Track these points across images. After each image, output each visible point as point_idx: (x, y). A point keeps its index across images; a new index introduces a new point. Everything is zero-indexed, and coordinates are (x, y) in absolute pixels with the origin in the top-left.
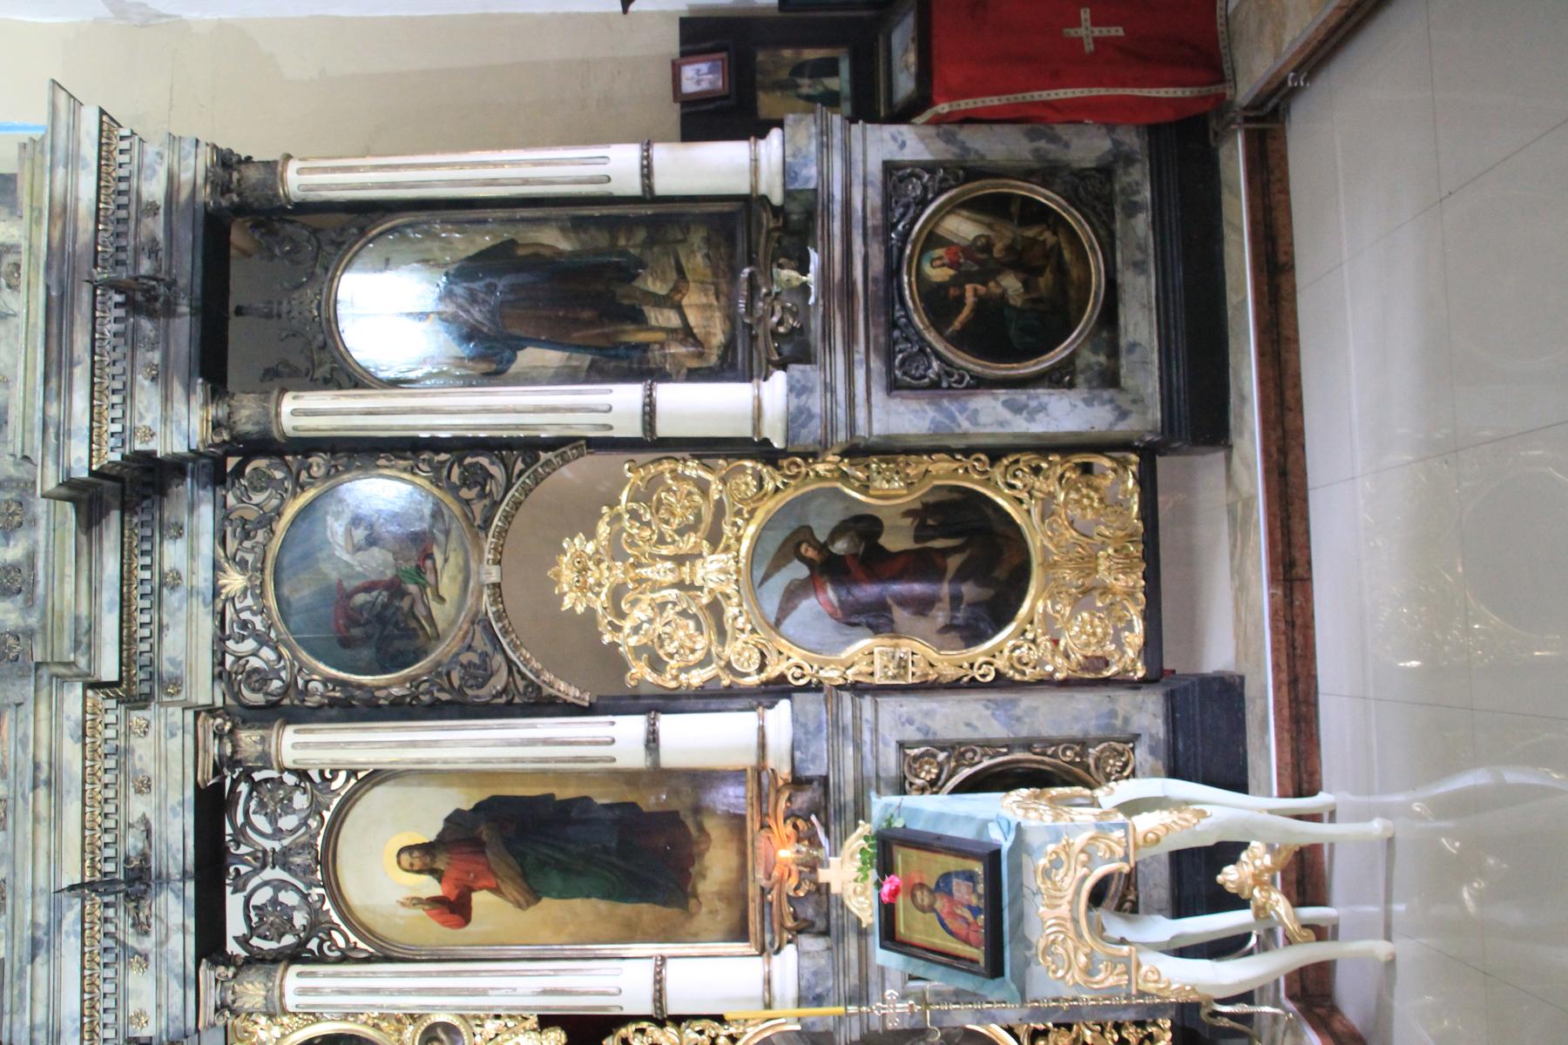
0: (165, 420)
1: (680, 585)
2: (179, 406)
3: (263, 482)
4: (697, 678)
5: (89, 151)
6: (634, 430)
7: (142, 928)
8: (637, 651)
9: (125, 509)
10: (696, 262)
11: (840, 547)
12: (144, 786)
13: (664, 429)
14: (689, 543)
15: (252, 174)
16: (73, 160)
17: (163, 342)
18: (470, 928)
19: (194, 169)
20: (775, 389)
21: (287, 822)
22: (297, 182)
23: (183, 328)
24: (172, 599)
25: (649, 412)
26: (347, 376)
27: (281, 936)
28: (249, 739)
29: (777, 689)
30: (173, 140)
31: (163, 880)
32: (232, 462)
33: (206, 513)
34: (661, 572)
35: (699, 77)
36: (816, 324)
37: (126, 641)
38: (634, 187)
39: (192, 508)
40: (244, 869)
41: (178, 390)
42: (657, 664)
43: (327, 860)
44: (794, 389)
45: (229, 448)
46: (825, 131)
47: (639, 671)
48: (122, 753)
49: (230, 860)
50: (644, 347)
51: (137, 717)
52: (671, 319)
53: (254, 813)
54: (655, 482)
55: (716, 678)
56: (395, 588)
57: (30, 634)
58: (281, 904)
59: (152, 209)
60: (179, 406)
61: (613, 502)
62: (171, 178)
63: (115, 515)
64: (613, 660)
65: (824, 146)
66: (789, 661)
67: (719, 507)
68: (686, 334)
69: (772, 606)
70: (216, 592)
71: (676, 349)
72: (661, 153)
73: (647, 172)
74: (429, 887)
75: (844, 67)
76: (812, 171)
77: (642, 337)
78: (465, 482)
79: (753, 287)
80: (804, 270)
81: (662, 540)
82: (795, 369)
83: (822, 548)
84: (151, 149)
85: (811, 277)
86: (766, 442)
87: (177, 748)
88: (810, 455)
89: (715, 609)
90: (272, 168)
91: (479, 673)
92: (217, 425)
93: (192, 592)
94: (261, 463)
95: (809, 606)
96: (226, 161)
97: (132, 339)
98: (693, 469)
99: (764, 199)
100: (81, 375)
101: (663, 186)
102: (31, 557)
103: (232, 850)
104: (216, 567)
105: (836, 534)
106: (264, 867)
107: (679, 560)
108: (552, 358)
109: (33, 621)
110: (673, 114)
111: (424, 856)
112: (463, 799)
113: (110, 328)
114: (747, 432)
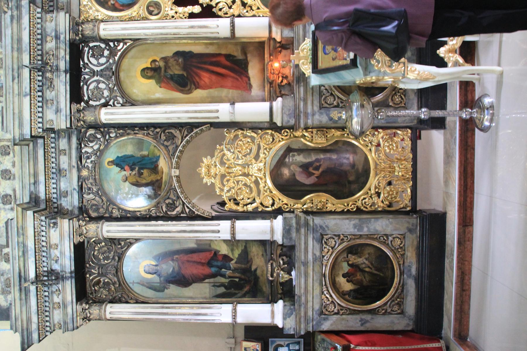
21: (103, 60)
27: (100, 99)
40: (87, 77)
43: (116, 74)
49: (83, 73)
53: (91, 57)
58: (99, 88)
103: (83, 70)
106: (94, 76)
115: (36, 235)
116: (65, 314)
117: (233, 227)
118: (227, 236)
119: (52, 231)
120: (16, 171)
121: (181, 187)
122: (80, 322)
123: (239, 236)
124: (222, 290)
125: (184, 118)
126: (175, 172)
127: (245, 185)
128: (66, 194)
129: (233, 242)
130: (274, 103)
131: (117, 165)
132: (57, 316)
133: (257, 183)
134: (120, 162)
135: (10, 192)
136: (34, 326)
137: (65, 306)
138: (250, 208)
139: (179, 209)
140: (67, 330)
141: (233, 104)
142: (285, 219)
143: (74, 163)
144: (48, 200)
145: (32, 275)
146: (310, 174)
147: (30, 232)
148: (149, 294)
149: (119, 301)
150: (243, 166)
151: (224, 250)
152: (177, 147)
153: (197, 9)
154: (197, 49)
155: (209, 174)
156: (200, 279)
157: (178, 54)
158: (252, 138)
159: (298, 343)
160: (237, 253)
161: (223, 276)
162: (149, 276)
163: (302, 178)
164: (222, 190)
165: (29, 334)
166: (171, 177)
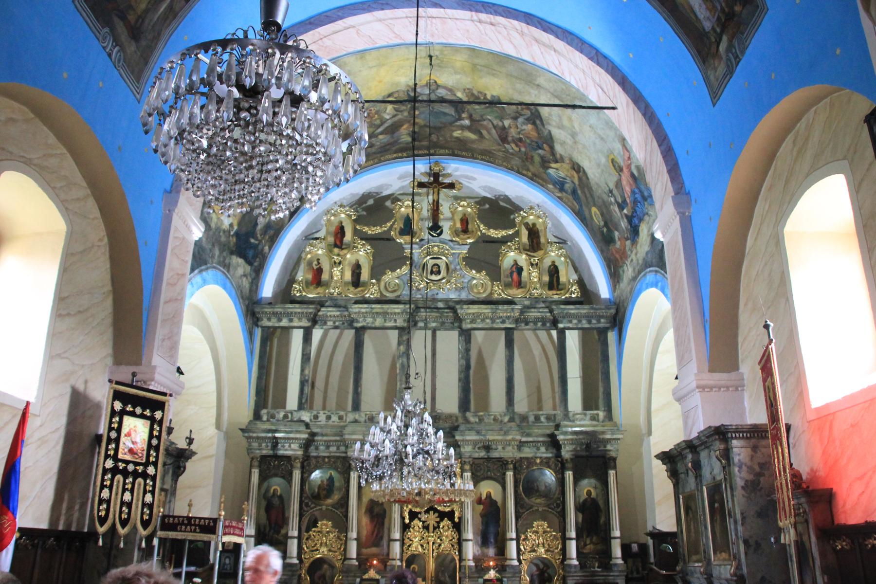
0: (568, 451)
1: (539, 544)
2: (570, 453)
3: (556, 465)
4: (522, 547)
5: (615, 437)
6: (567, 536)
7: (479, 448)
8: (527, 537)
9: (551, 441)
10: (599, 547)
11: (546, 575)
12: (504, 448)
13: (567, 542)
14: (546, 546)
15: (612, 464)
16: (613, 434)
17: (581, 450)
18: (476, 505)
19: (613, 454)
20: (575, 562)
22: (612, 473)
23: (584, 453)
24: (535, 449)
25: (571, 539)
26: (576, 481)
28: (511, 466)
29: (520, 562)
30: (617, 450)
31: (488, 452)
32: (559, 459)
33: (550, 455)
34: (541, 540)
35: (635, 547)
36: (588, 570)
37: (527, 442)
38: (612, 535)
39: (552, 453)
41: (573, 453)
42: (524, 540)
44: (575, 566)
45: (562, 460)
46: (622, 571)
47: (523, 537)
48: (509, 445)
50: (583, 537)
51: (516, 447)
52: (588, 542)
54: (557, 540)
55: (521, 550)
56: (538, 491)
57: (528, 422)
59: (605, 447)
60: (570, 453)
61: (554, 531)
62: (610, 450)
63: (549, 439)
64: (525, 532)
65: (620, 571)
66: (525, 567)
67: (553, 552)
68: (585, 545)
69: (535, 561)
70: (537, 458)
71: (582, 544)
72: (618, 541)
73: (615, 538)
74: (484, 496)
75: (638, 576)
76: (616, 569)
77: (585, 537)
78: (557, 504)
79: (594, 558)
80: (598, 567)
81: (547, 541)
82: (579, 566)
83: (546, 571)
84: (616, 446)
85: (596, 569)
86: (565, 560)
87: (511, 455)
88: (563, 569)
89: (534, 551)
90: (615, 468)
91: (522, 506)
92: (566, 460)
93: (536, 453)
94: (560, 465)
95: (535, 569)
96: (614, 459)
97: (582, 444)
98: (560, 547)
99: (611, 560)
100: (575, 437)
101: (613, 541)
102: (542, 422)
104: (541, 458)
105: (548, 574)
107: (543, 544)
108: (580, 519)
109: (530, 423)
110: (626, 542)
111: (489, 496)
112: (500, 503)
113: (583, 441)
114: (568, 556)
115: (296, 439)
116: (256, 449)
117: (294, 537)
118: (290, 534)
119: (298, 445)
120: (330, 422)
121: (317, 510)
122: (252, 455)
123: (289, 541)
124: (262, 529)
125: (350, 515)
126: (324, 508)
127: (316, 544)
128: (317, 448)
129: (287, 537)
130: (355, 561)
131: (330, 477)
132: (255, 445)
133: (317, 550)
134: (331, 479)
135: (319, 419)
136: (251, 434)
137: (259, 449)
138: (304, 546)
139: (305, 509)
140: (248, 449)
141: (355, 539)
142: (296, 564)
143: (332, 454)
144: (314, 441)
145: (277, 435)
146: (319, 578)
147: (298, 436)
148: (263, 491)
149: (260, 475)
150: (326, 543)
151: (283, 532)
152: (337, 509)
153: (407, 521)
154: (386, 521)
155: (322, 525)
156: (269, 518)
157: (385, 511)
158: (340, 548)
159: (230, 569)
160: (281, 538)
161: (270, 531)
162: (272, 491)
163: (318, 574)
164: (314, 531)
165: (248, 432)
166: (322, 505)
